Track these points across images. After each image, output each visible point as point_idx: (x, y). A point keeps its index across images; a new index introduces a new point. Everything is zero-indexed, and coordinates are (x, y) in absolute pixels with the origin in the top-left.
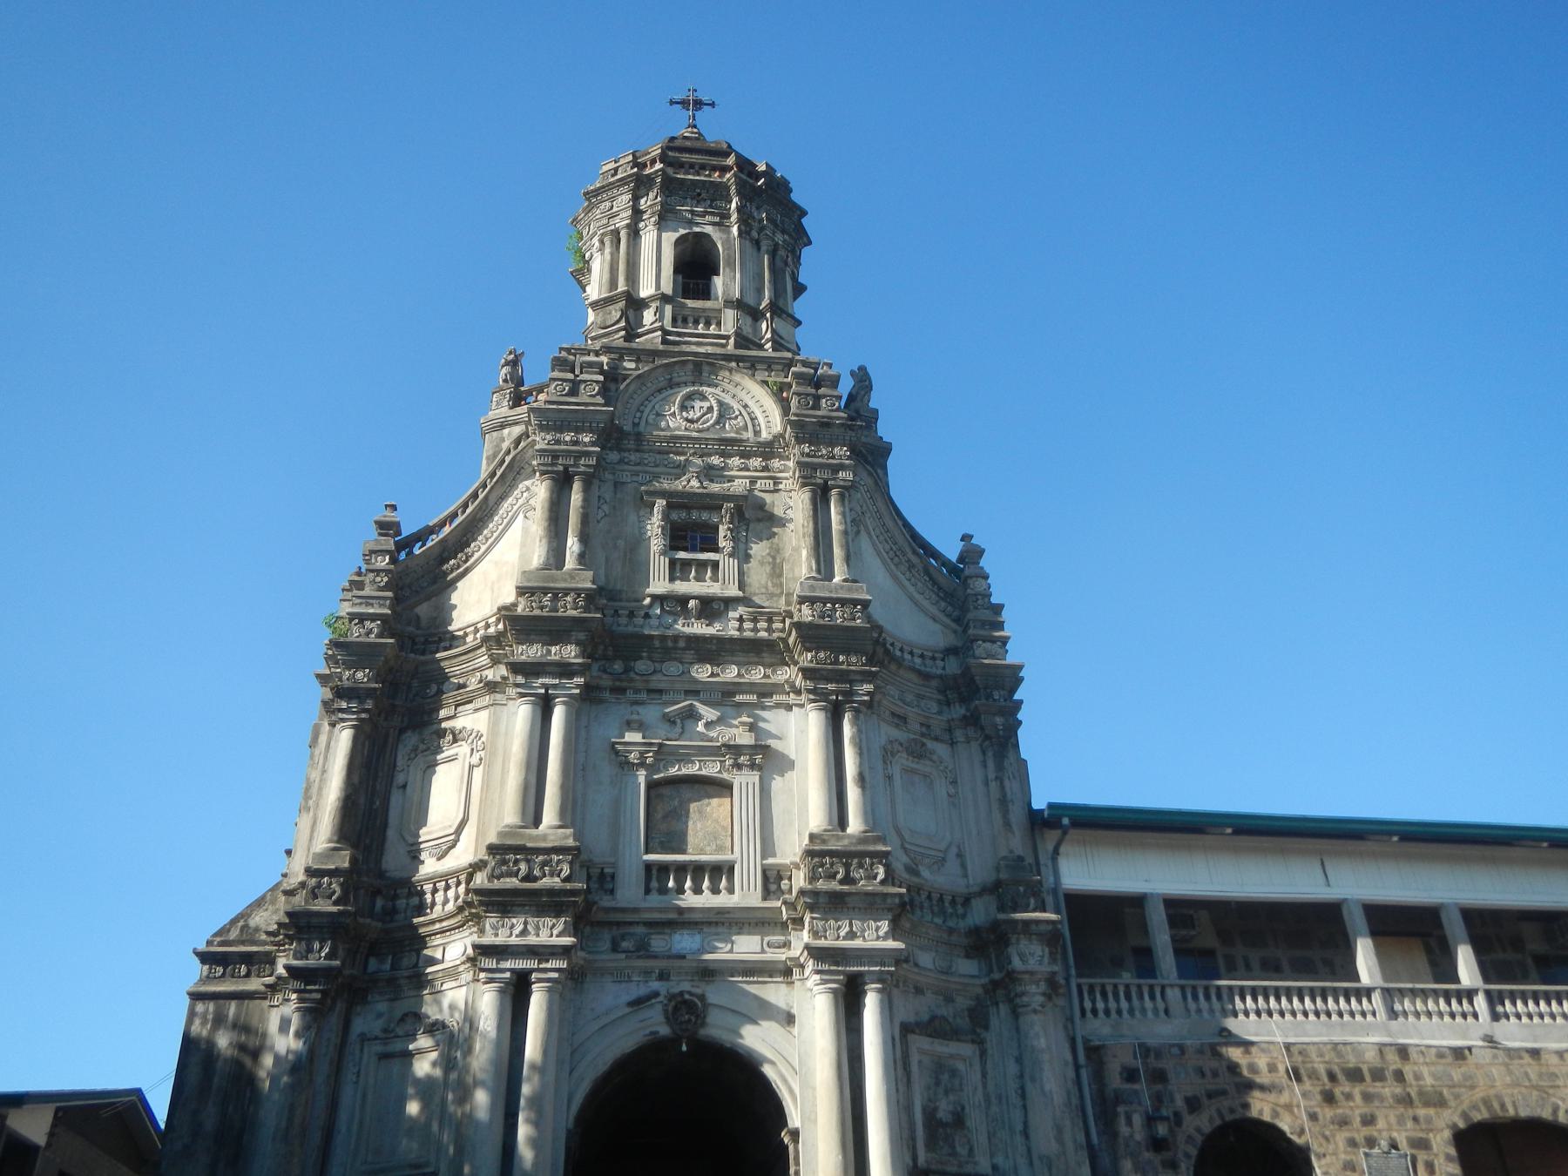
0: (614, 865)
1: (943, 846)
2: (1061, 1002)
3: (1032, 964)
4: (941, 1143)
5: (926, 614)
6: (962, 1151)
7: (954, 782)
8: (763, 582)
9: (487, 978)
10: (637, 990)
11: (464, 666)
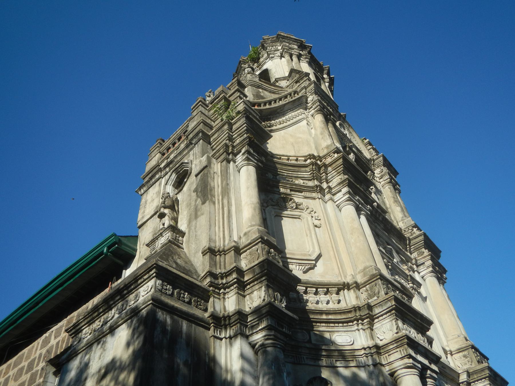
9: (413, 364)
11: (290, 173)
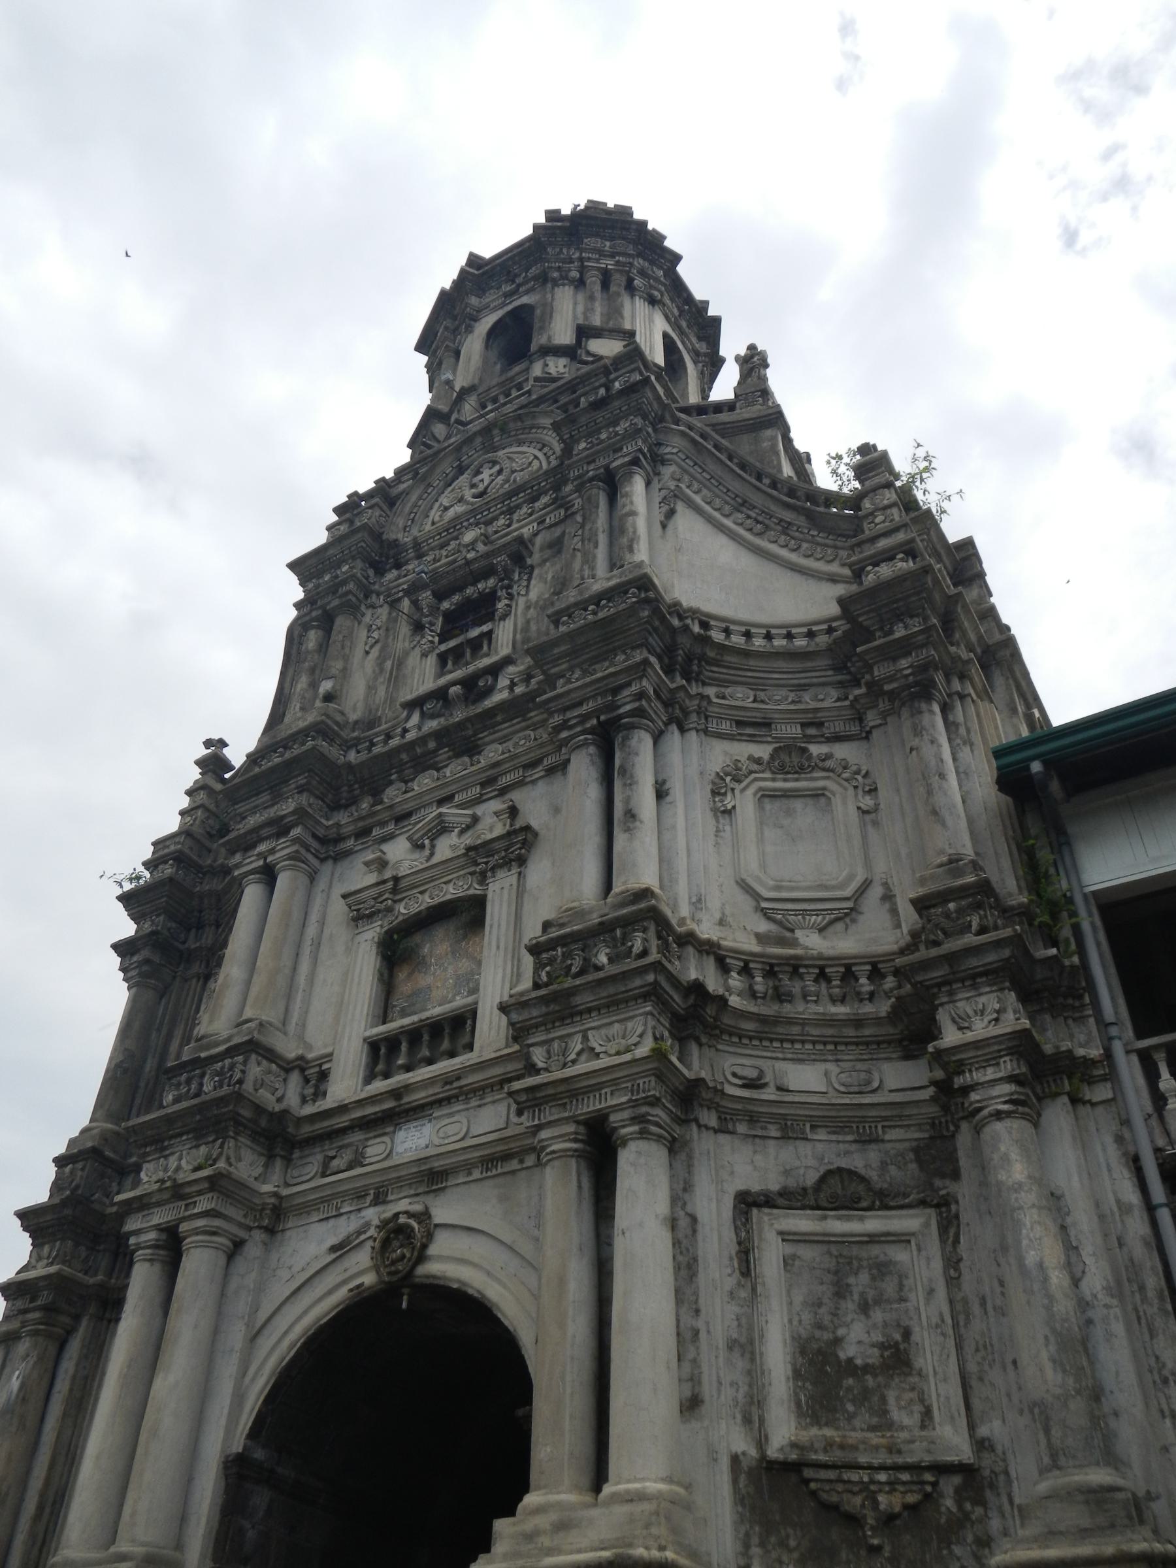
0: (329, 1056)
1: (848, 892)
2: (1102, 1092)
3: (981, 1029)
4: (850, 1408)
5: (820, 579)
6: (905, 1418)
7: (873, 791)
8: (543, 629)
10: (343, 1228)
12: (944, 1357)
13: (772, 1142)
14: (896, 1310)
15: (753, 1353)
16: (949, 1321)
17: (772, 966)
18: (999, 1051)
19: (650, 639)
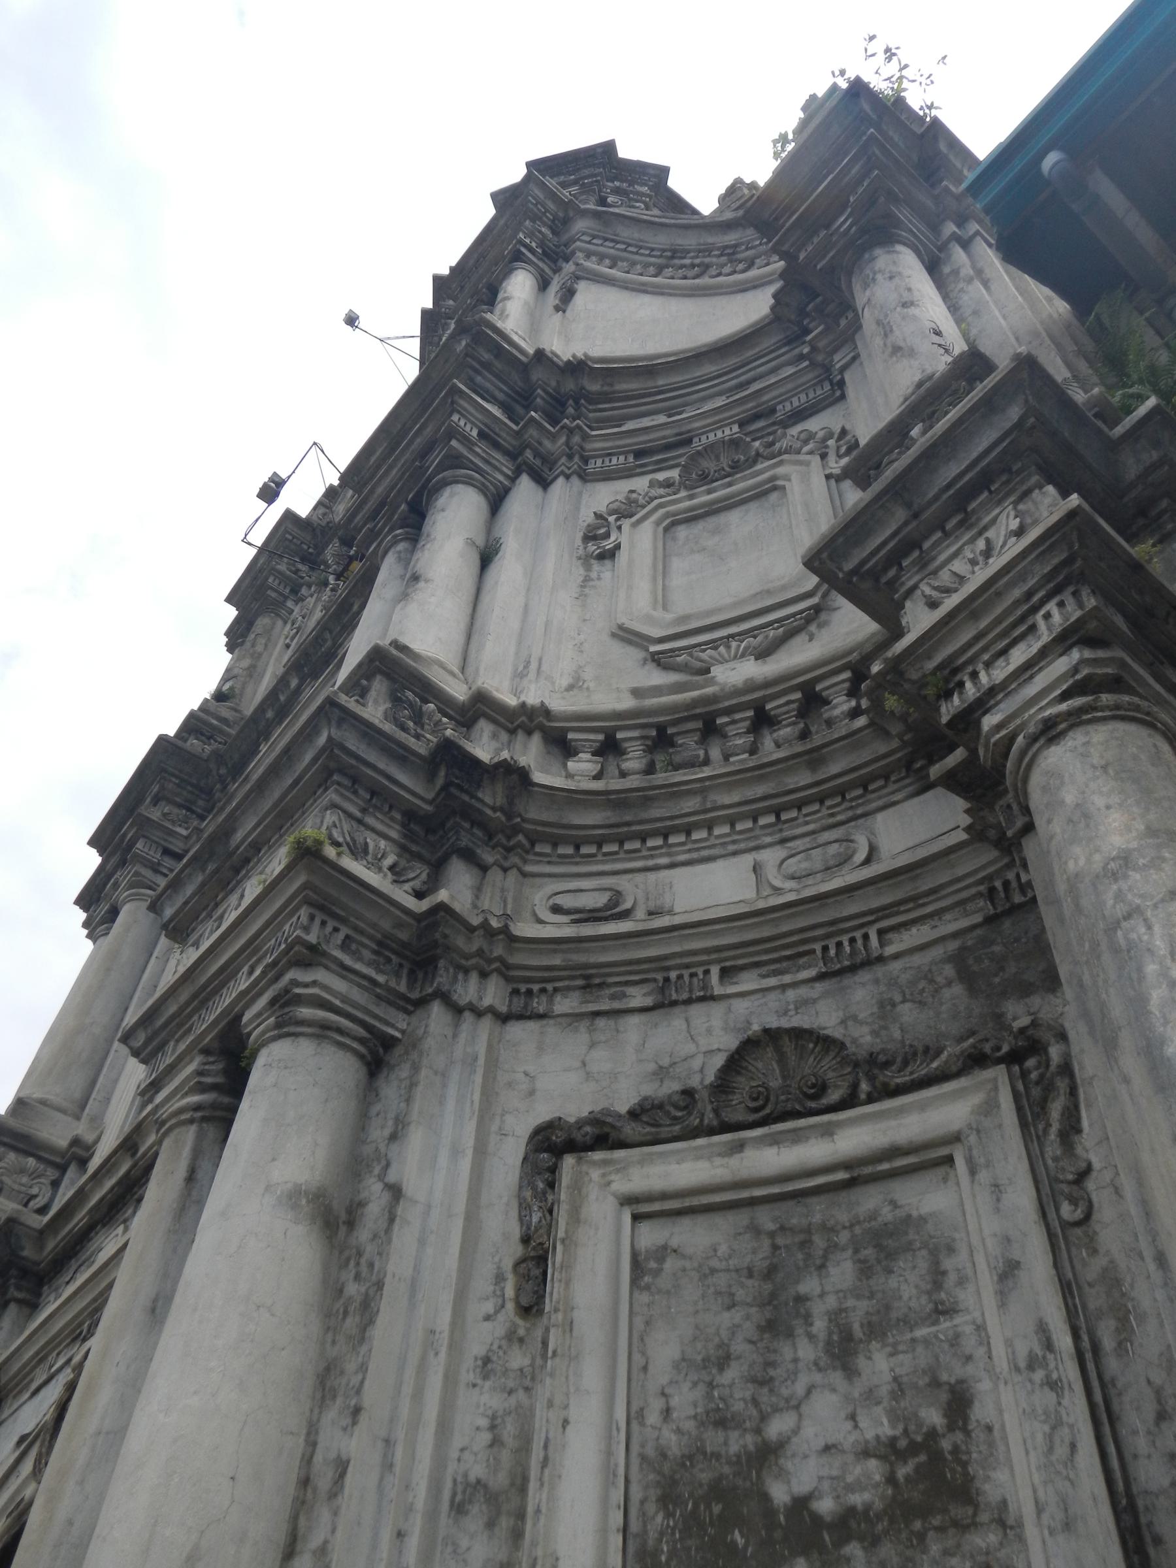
12: (1061, 1451)
13: (634, 1020)
14: (926, 1342)
15: (521, 1516)
16: (1064, 1341)
17: (661, 729)
18: (1029, 594)
19: (479, 379)
